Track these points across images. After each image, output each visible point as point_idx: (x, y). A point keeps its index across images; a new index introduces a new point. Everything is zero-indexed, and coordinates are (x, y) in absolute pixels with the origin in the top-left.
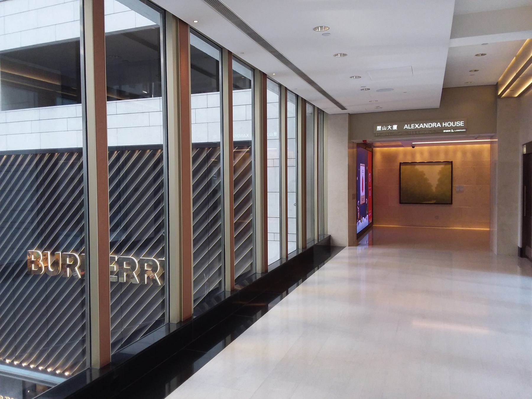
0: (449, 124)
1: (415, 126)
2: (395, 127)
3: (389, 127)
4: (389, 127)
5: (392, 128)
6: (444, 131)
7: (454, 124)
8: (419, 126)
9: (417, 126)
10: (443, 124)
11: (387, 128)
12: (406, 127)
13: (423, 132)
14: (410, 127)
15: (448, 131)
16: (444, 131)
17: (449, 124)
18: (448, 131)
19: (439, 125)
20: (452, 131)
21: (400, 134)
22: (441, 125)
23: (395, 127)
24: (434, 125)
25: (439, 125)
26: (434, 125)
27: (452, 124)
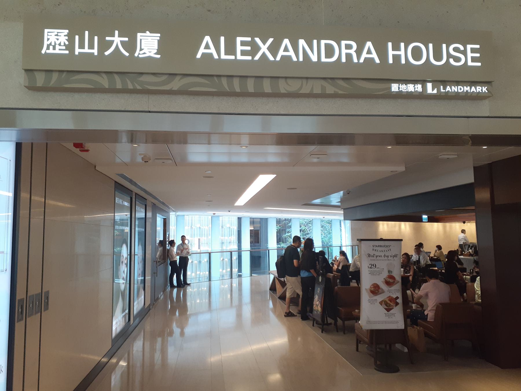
0: (417, 54)
1: (256, 49)
2: (148, 44)
3: (117, 40)
4: (117, 40)
5: (131, 46)
6: (395, 87)
7: (438, 56)
8: (274, 49)
9: (264, 48)
10: (391, 53)
11: (104, 45)
12: (206, 47)
13: (294, 86)
14: (231, 49)
15: (411, 88)
16: (395, 87)
17: (417, 54)
18: (411, 88)
19: (370, 52)
21: (176, 84)
22: (382, 53)
23: (148, 44)
24: (345, 50)
25: (370, 52)
26: (345, 50)
27: (427, 52)
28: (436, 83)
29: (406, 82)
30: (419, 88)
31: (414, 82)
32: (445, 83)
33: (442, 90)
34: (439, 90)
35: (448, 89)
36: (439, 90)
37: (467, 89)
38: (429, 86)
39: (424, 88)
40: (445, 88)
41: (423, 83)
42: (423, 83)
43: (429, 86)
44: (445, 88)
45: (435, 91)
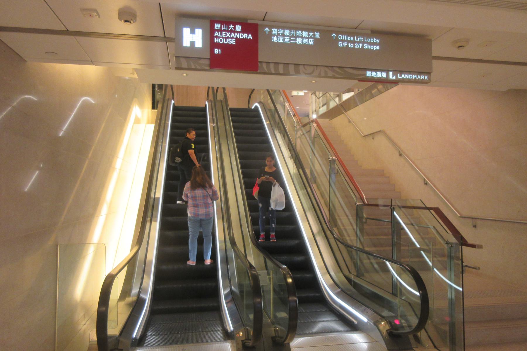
6: (369, 74)
15: (379, 75)
16: (369, 74)
18: (379, 75)
20: (391, 76)
28: (395, 72)
29: (376, 70)
30: (384, 75)
31: (382, 71)
32: (401, 72)
33: (399, 77)
34: (397, 77)
35: (403, 76)
36: (397, 77)
37: (415, 77)
38: (391, 74)
39: (388, 75)
40: (401, 76)
41: (388, 72)
42: (388, 72)
43: (391, 74)
44: (401, 76)
45: (394, 78)
